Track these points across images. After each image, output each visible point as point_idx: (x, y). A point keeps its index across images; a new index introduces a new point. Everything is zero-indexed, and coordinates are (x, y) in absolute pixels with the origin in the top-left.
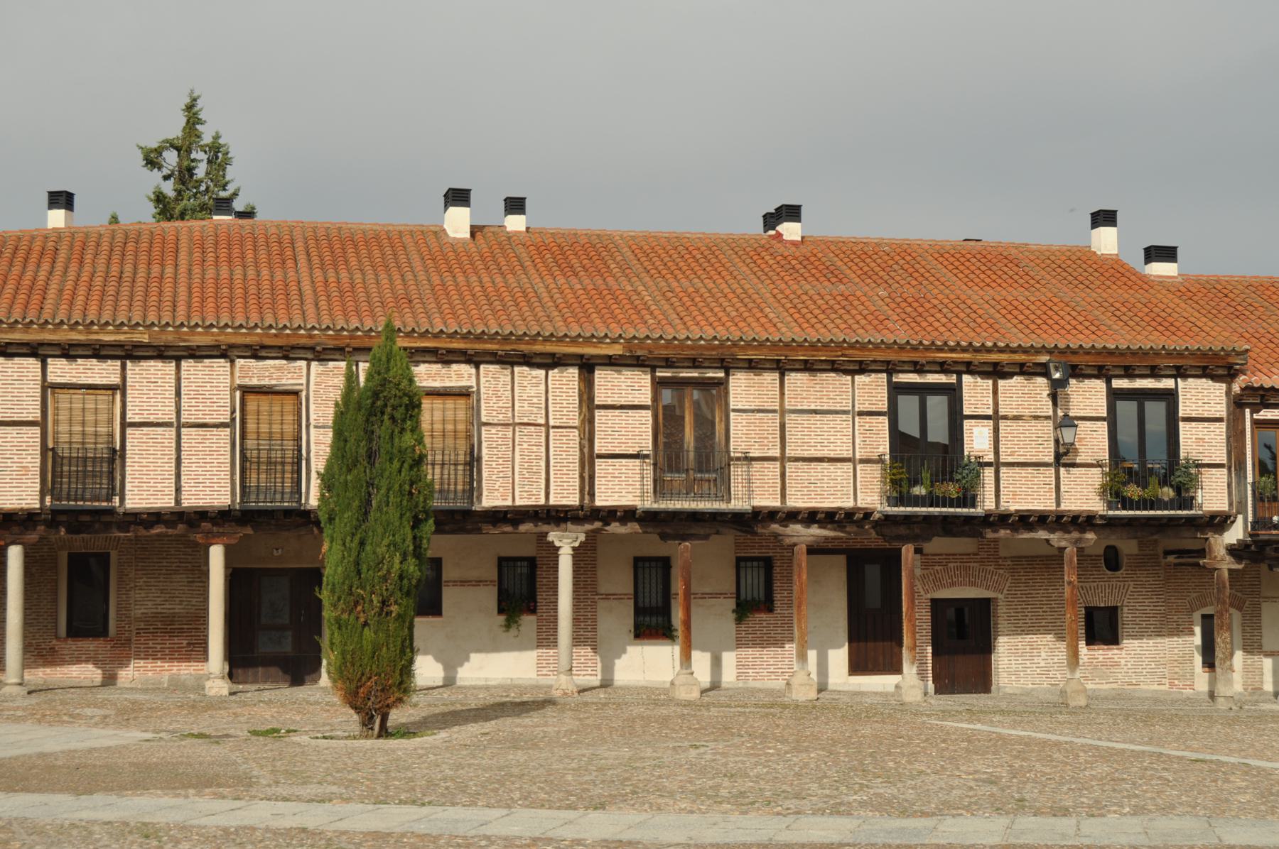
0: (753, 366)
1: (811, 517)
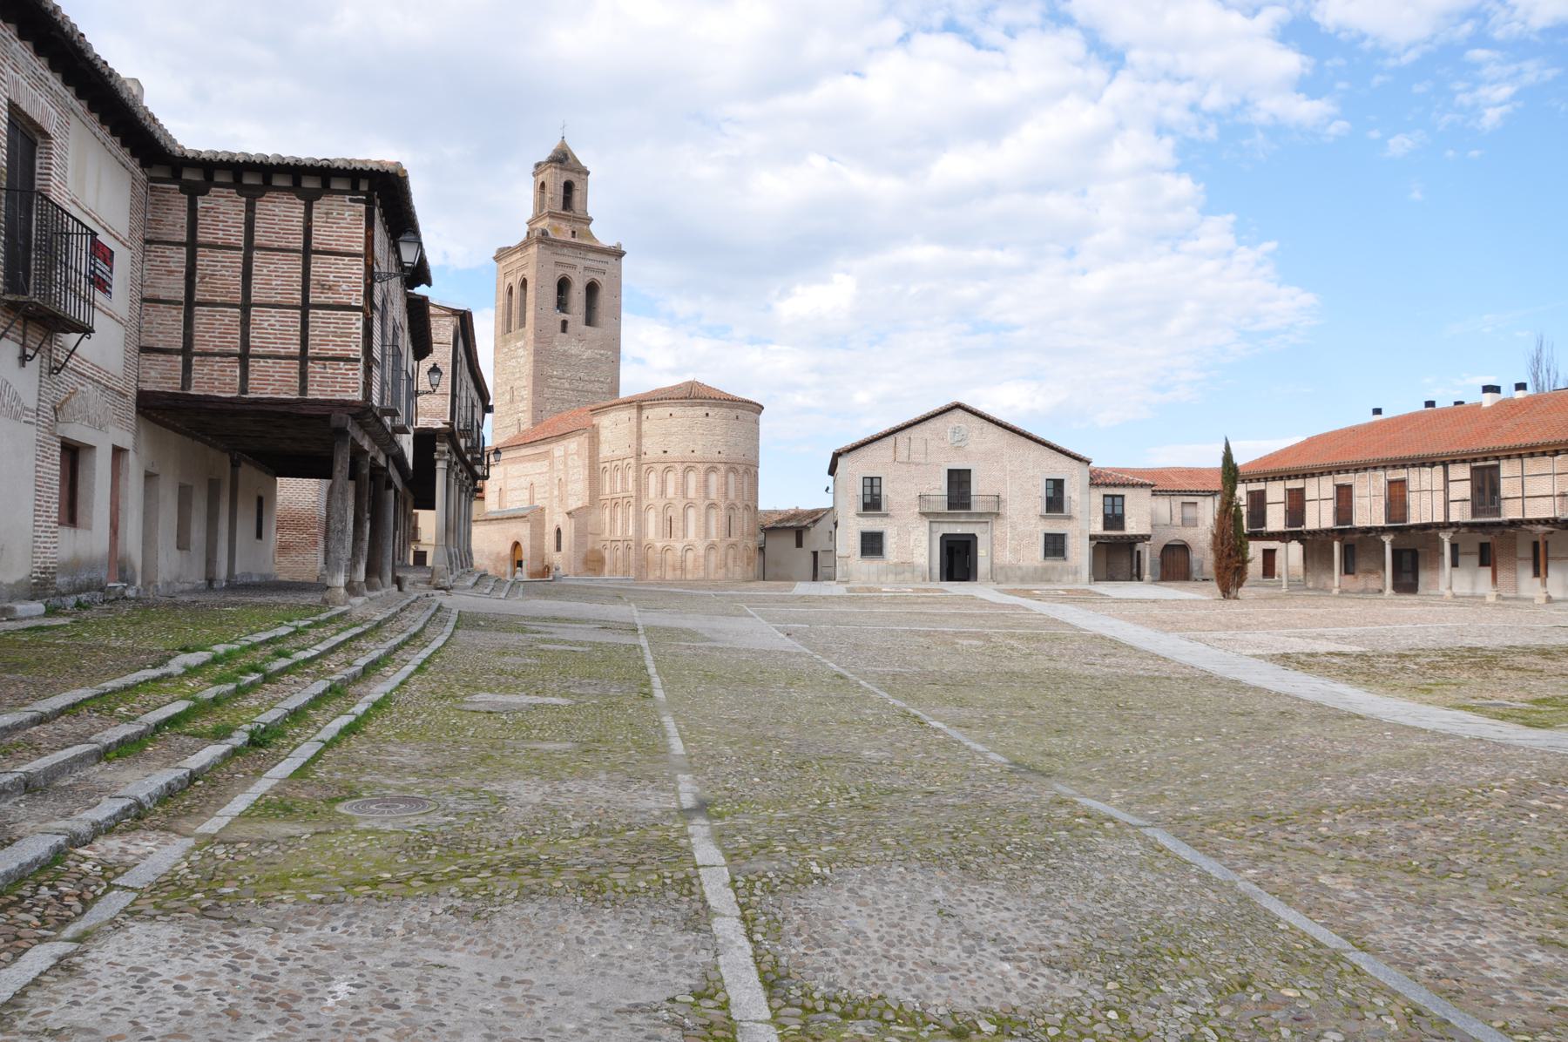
0: (1508, 457)
1: (1538, 521)
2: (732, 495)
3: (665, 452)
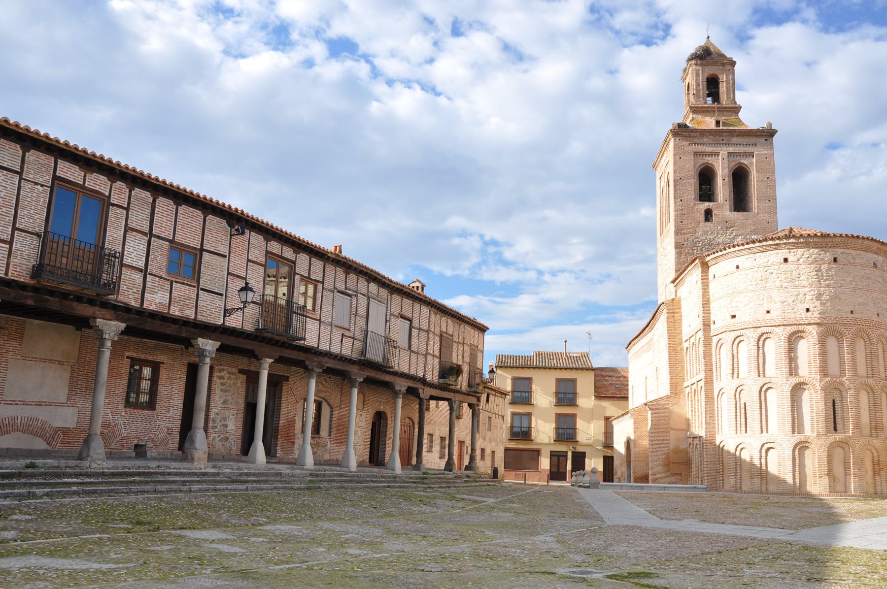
2: (834, 368)
3: (734, 317)
